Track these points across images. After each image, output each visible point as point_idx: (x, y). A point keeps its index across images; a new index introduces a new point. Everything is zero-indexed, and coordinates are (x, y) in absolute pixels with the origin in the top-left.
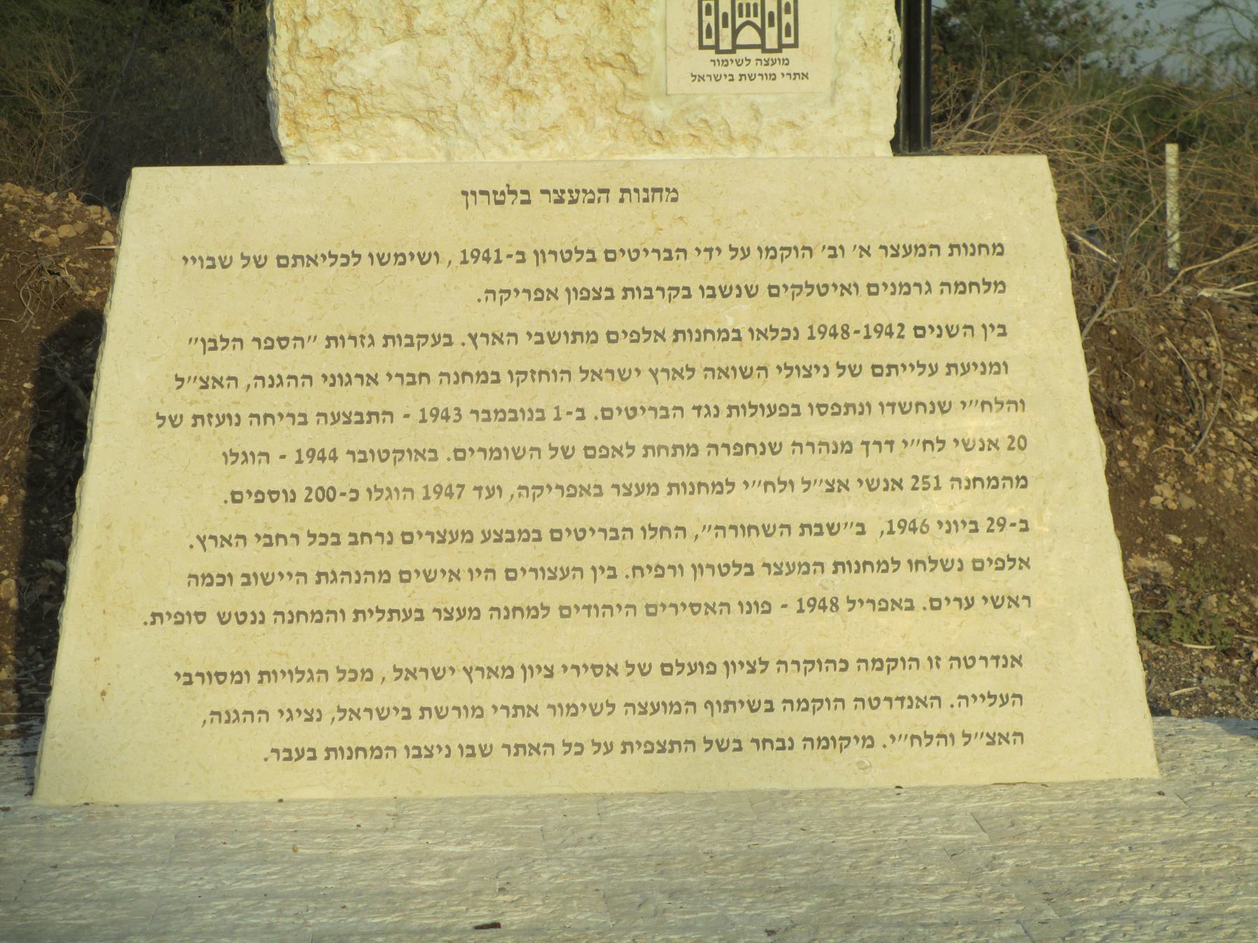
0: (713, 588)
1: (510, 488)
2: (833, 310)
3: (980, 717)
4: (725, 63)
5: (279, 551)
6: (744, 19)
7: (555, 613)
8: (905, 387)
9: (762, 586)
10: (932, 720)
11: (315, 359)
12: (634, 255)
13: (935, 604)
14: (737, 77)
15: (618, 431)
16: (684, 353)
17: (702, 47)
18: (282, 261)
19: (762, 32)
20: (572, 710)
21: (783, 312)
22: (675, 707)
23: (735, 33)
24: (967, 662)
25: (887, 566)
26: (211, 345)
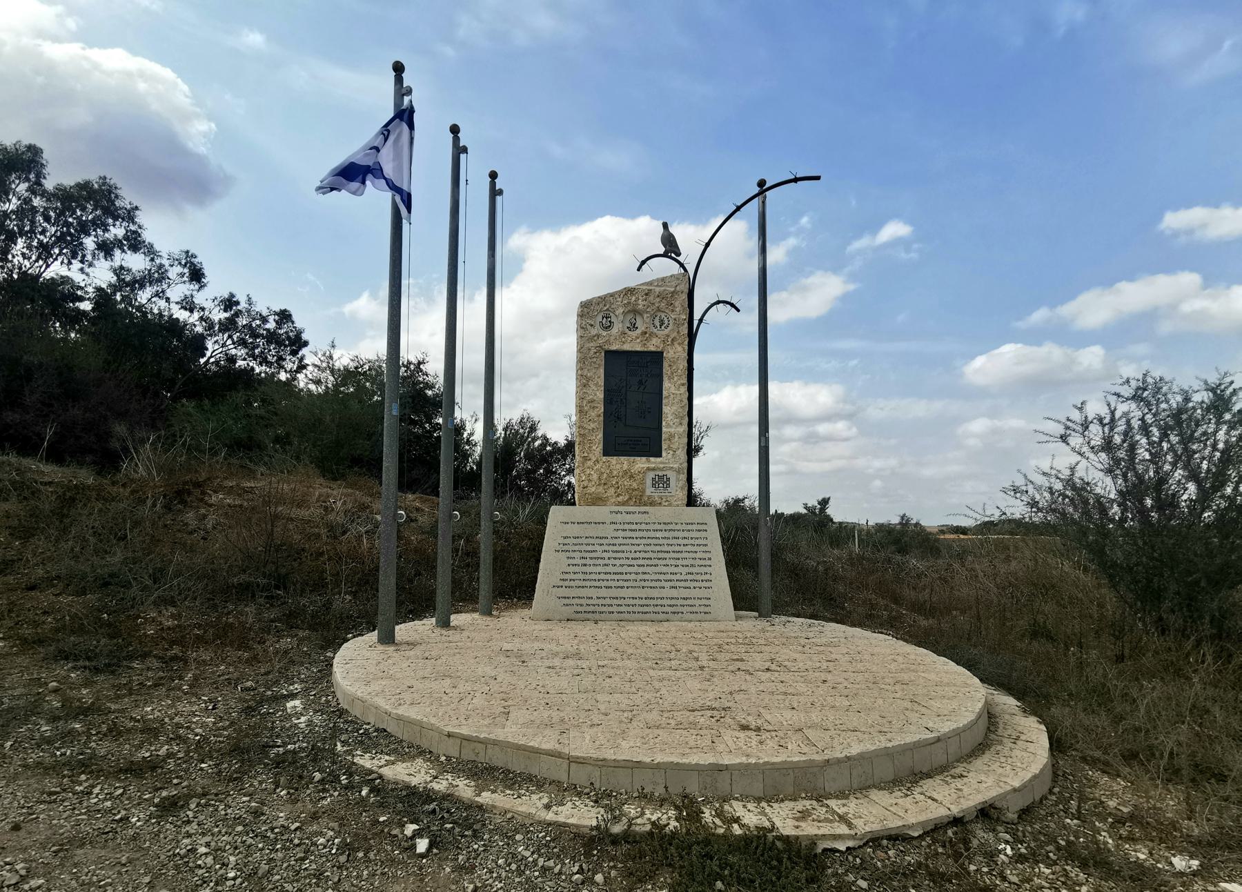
2: (676, 534)
3: (703, 609)
8: (689, 548)
10: (694, 609)
11: (584, 541)
15: (638, 555)
16: (649, 541)
21: (666, 534)
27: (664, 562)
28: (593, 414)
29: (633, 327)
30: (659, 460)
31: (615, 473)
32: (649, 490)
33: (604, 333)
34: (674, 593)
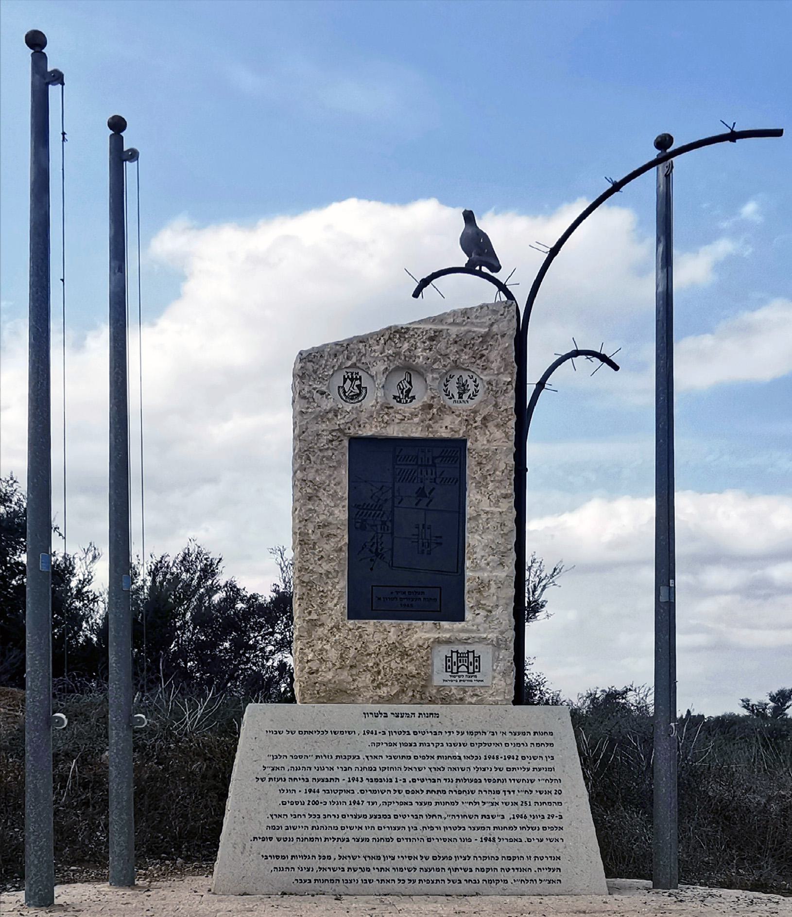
2: (493, 751)
4: (454, 677)
7: (395, 840)
12: (423, 733)
21: (474, 751)
23: (458, 668)
28: (328, 547)
30: (458, 625)
31: (372, 648)
32: (440, 677)
33: (348, 407)
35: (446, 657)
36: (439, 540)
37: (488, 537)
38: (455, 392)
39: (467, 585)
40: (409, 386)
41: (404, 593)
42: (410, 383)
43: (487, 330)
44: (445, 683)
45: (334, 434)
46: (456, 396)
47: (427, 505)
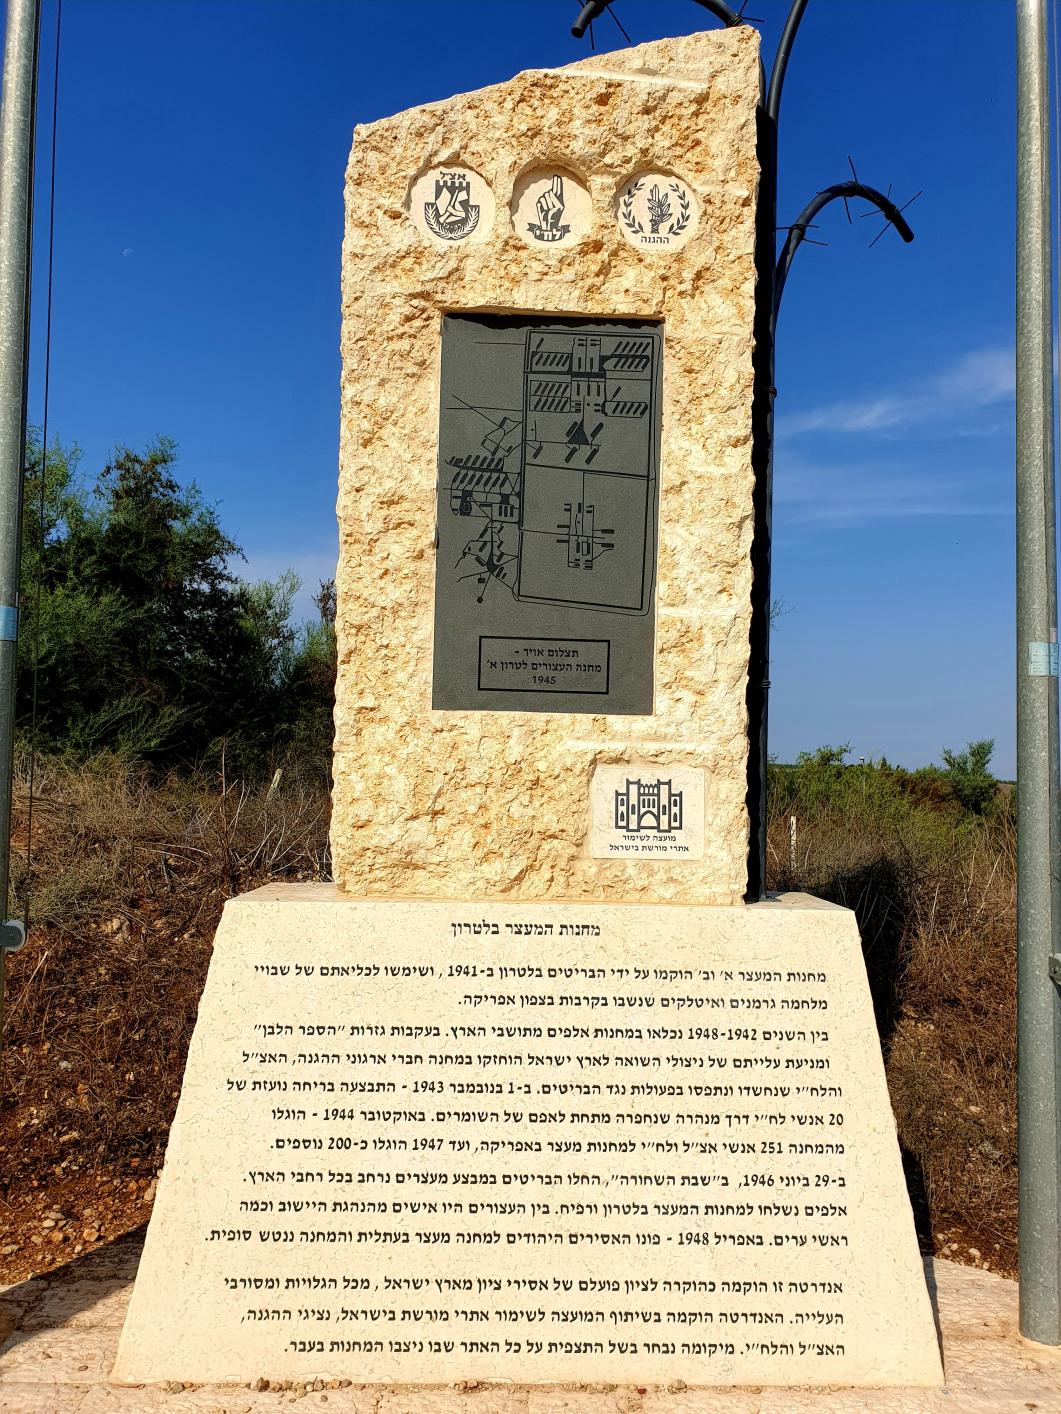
0: (615, 1224)
1: (475, 1143)
2: (705, 1018)
3: (814, 1333)
5: (307, 1184)
6: (646, 809)
7: (504, 1239)
9: (653, 1223)
12: (569, 973)
13: (778, 1240)
14: (640, 848)
15: (554, 1103)
17: (617, 827)
18: (324, 971)
19: (658, 818)
20: (514, 1316)
21: (669, 1018)
22: (588, 1316)
23: (640, 818)
24: (803, 1288)
25: (744, 1209)
26: (270, 1030)
27: (659, 1133)
28: (397, 547)
29: (553, 223)
30: (639, 724)
31: (475, 772)
32: (604, 837)
33: (441, 244)
34: (696, 1263)
35: (617, 794)
36: (608, 539)
37: (702, 530)
38: (644, 217)
39: (661, 637)
40: (558, 205)
41: (541, 652)
42: (560, 198)
43: (705, 86)
44: (615, 854)
45: (415, 302)
46: (647, 227)
47: (588, 461)
